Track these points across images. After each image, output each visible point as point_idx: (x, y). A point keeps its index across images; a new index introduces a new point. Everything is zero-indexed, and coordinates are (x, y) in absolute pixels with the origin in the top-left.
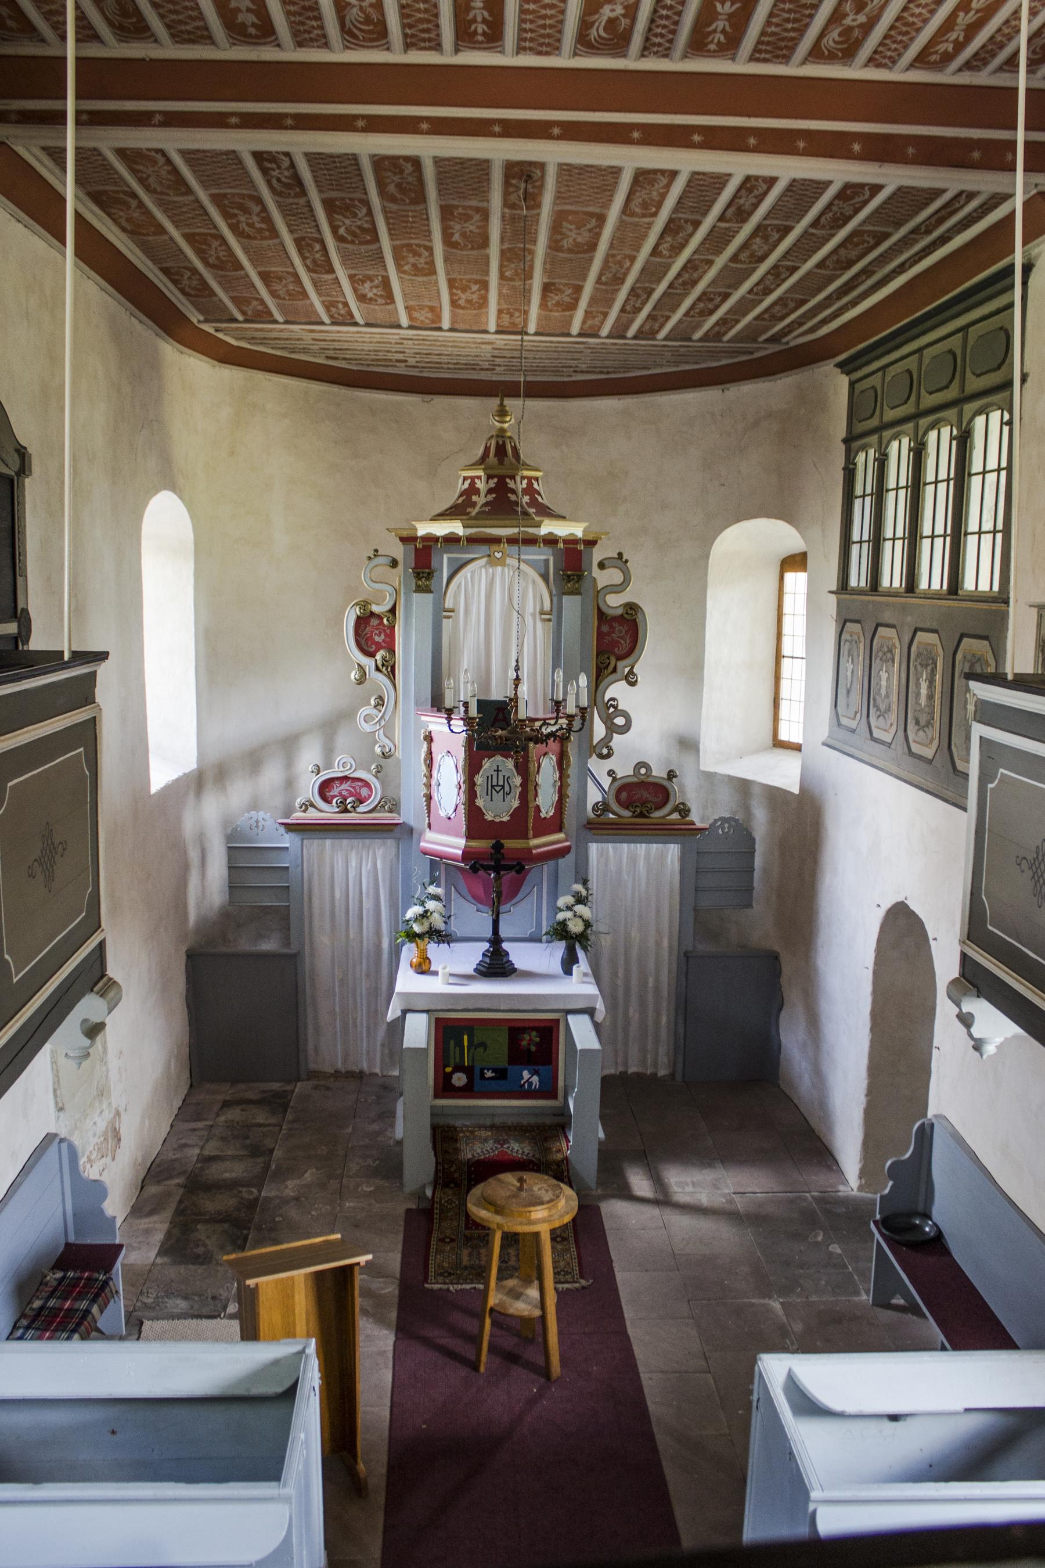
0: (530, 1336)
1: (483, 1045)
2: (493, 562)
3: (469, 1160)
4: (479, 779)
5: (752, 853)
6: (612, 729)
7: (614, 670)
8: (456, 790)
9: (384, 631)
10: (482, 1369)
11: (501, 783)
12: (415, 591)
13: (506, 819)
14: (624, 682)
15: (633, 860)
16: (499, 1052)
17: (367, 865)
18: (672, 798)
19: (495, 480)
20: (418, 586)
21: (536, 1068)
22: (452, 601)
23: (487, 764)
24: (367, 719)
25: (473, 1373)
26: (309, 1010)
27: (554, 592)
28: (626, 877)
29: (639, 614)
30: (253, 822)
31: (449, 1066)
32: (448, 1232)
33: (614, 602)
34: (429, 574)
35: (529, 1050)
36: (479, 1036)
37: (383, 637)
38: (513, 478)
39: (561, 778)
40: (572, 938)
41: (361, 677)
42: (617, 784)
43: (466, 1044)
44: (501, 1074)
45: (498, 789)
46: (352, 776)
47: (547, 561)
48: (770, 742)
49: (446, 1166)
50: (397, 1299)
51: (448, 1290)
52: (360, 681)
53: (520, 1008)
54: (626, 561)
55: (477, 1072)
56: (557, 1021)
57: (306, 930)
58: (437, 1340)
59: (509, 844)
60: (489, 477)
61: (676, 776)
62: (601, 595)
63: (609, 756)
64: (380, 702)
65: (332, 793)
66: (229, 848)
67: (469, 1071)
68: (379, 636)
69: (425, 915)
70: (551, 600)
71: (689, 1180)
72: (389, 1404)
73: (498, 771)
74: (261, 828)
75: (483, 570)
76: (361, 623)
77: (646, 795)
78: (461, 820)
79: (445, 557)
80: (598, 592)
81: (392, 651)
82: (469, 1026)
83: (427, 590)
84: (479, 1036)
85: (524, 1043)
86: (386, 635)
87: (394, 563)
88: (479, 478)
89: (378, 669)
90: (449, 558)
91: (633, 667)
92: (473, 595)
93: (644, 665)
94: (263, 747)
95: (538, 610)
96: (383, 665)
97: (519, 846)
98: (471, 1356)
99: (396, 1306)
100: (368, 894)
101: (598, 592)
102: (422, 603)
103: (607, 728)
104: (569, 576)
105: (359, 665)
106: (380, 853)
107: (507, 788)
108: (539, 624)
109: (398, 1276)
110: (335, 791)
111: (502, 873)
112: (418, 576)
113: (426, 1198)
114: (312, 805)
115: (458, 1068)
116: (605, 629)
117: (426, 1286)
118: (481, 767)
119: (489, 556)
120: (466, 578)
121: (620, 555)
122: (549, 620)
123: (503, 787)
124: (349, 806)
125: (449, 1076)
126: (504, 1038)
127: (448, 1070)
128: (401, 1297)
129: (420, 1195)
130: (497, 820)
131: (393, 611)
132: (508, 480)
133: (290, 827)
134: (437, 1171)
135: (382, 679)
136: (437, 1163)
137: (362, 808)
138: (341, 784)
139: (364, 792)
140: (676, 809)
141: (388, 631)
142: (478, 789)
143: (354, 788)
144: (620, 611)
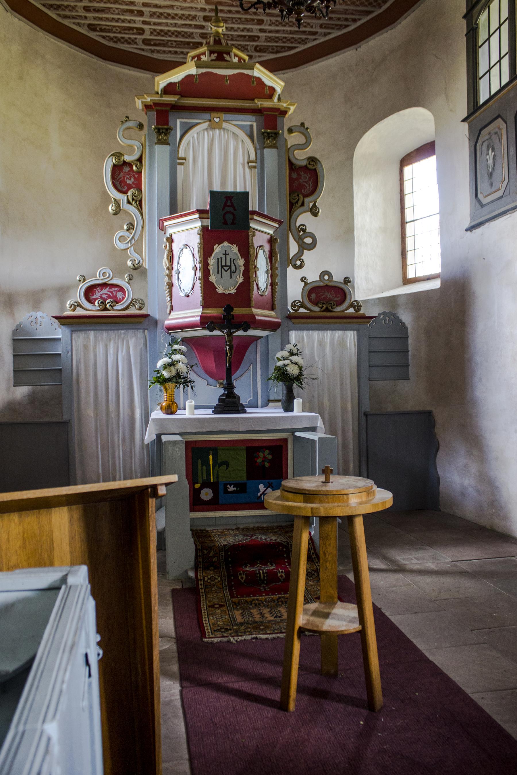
0: (332, 671)
1: (226, 463)
2: (213, 126)
3: (225, 545)
4: (212, 261)
5: (407, 338)
6: (303, 247)
7: (303, 204)
8: (193, 272)
9: (134, 176)
10: (292, 706)
11: (228, 264)
12: (156, 144)
13: (233, 292)
14: (309, 213)
15: (321, 344)
16: (238, 470)
17: (122, 352)
18: (348, 297)
19: (216, 55)
20: (159, 140)
21: (271, 481)
22: (183, 152)
23: (218, 249)
24: (122, 239)
25: (281, 714)
26: (78, 465)
27: (258, 147)
28: (317, 359)
29: (318, 165)
30: (32, 319)
31: (197, 483)
32: (216, 601)
33: (300, 157)
34: (167, 130)
35: (264, 465)
36: (222, 456)
37: (132, 180)
38: (229, 54)
39: (271, 269)
40: (290, 379)
41: (117, 208)
42: (308, 287)
43: (211, 462)
44: (241, 488)
45: (226, 268)
46: (110, 282)
47: (251, 126)
48: (401, 282)
49: (205, 552)
50: (176, 654)
51: (229, 641)
52: (116, 213)
53: (256, 429)
54: (307, 129)
55: (221, 487)
56: (285, 440)
57: (75, 406)
58: (230, 685)
59: (237, 311)
60: (211, 52)
61: (350, 282)
62: (290, 151)
63: (301, 267)
64: (131, 227)
65: (94, 297)
66: (14, 340)
67: (214, 486)
68: (130, 179)
69: (172, 364)
70: (256, 153)
71: (411, 557)
72: (187, 756)
73: (226, 254)
74: (39, 324)
75: (206, 133)
76: (116, 169)
77: (329, 296)
78: (198, 295)
79: (178, 121)
80: (289, 149)
81: (140, 190)
82: (213, 447)
83: (165, 143)
84: (222, 456)
85: (259, 460)
86: (135, 179)
87: (141, 126)
88: (204, 54)
89: (129, 202)
90: (181, 122)
91: (315, 203)
92: (199, 149)
93: (322, 200)
94: (43, 291)
95: (246, 161)
96: (133, 199)
97: (244, 312)
98: (276, 695)
99: (176, 659)
100: (123, 374)
101: (289, 149)
102: (162, 152)
103: (299, 245)
104: (268, 134)
105: (115, 199)
106: (132, 342)
107: (233, 268)
108: (247, 170)
109: (173, 634)
110: (97, 295)
111: (232, 331)
112: (159, 131)
113: (190, 578)
114: (79, 305)
115: (206, 484)
116: (295, 176)
117: (205, 640)
118: (213, 251)
119: (210, 121)
120: (193, 137)
121: (303, 124)
122: (255, 167)
123: (230, 267)
124: (108, 306)
125: (199, 490)
126: (242, 456)
127: (197, 486)
128: (180, 652)
129: (184, 578)
130: (227, 292)
131: (140, 160)
132: (225, 55)
133: (62, 320)
134: (197, 557)
135: (132, 210)
136: (197, 550)
137: (118, 307)
138: (102, 289)
139: (120, 295)
140: (352, 305)
141: (136, 176)
142: (211, 268)
143: (111, 292)
144: (304, 163)
